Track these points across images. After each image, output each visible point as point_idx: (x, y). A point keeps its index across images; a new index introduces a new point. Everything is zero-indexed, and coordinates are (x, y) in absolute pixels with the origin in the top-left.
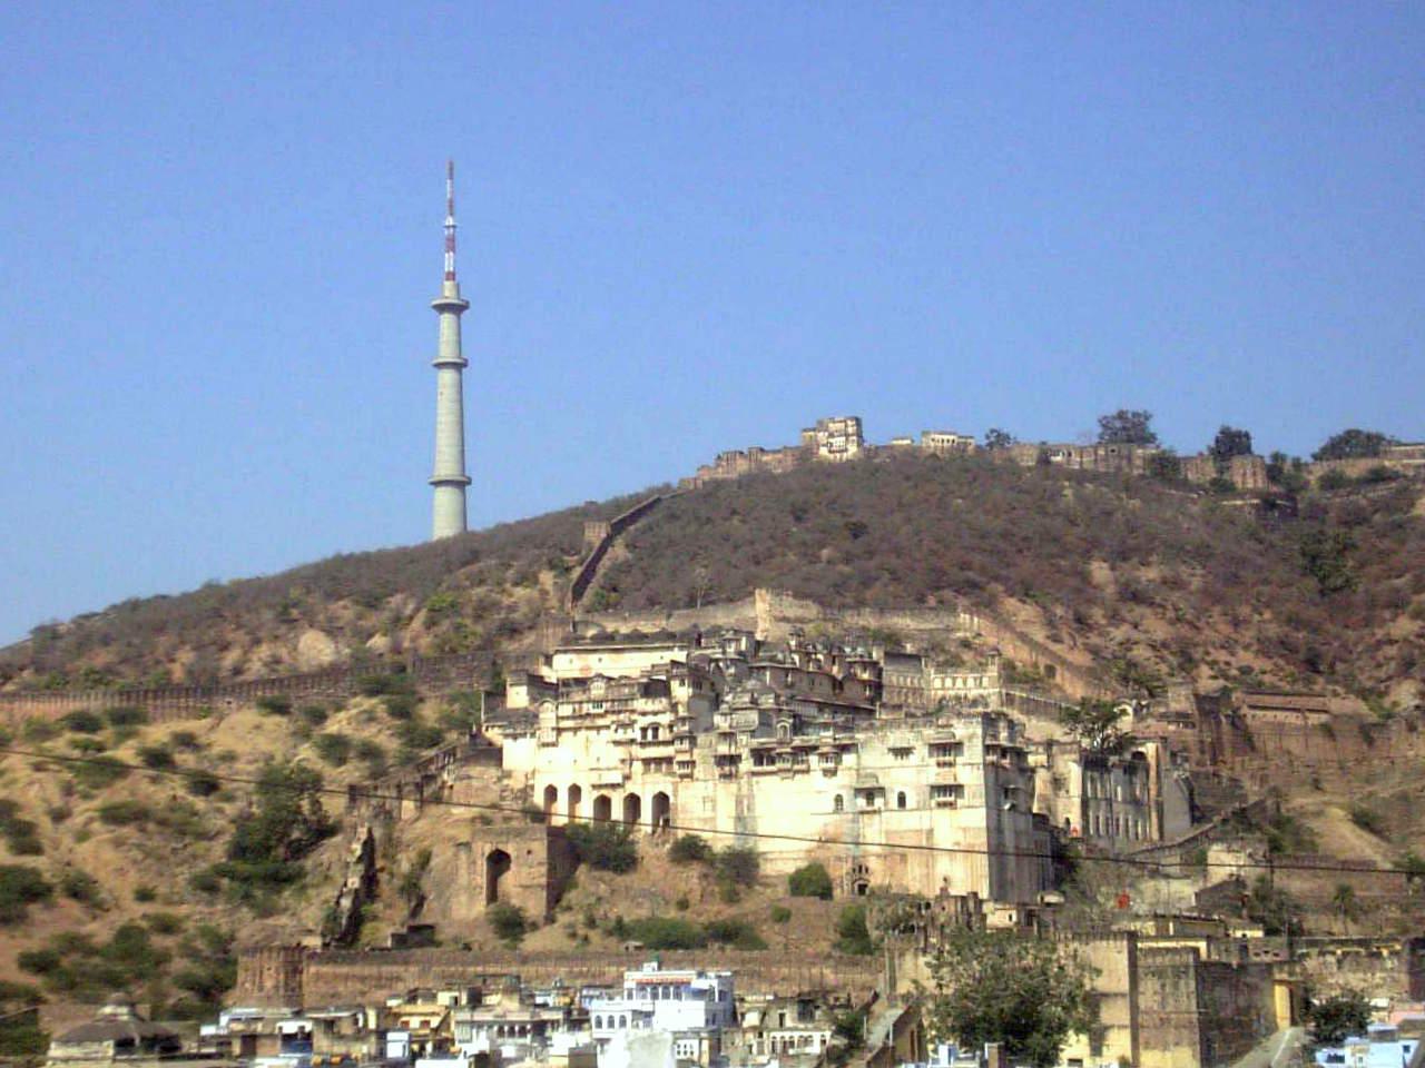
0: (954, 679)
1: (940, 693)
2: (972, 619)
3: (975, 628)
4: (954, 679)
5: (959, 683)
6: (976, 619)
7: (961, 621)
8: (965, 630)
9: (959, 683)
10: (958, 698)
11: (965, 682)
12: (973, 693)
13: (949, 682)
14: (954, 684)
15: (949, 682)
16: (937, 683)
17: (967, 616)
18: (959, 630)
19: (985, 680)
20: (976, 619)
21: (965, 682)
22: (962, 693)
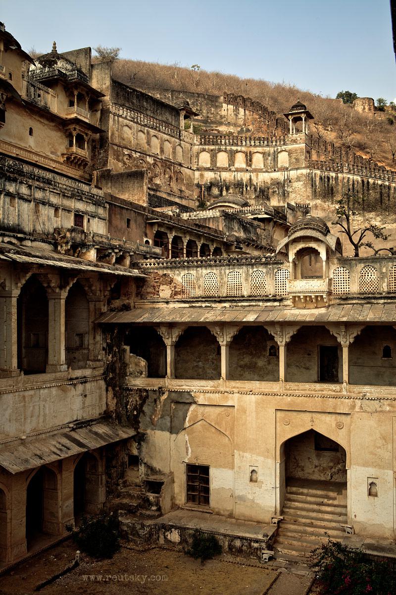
0: (232, 155)
1: (209, 176)
2: (236, 111)
3: (241, 122)
4: (232, 155)
5: (240, 161)
6: (241, 111)
7: (223, 113)
8: (229, 124)
9: (240, 161)
10: (239, 185)
11: (249, 160)
12: (263, 178)
13: (222, 159)
14: (232, 161)
15: (222, 159)
16: (205, 159)
17: (231, 107)
18: (221, 124)
19: (283, 159)
20: (241, 111)
21: (249, 160)
22: (245, 177)
